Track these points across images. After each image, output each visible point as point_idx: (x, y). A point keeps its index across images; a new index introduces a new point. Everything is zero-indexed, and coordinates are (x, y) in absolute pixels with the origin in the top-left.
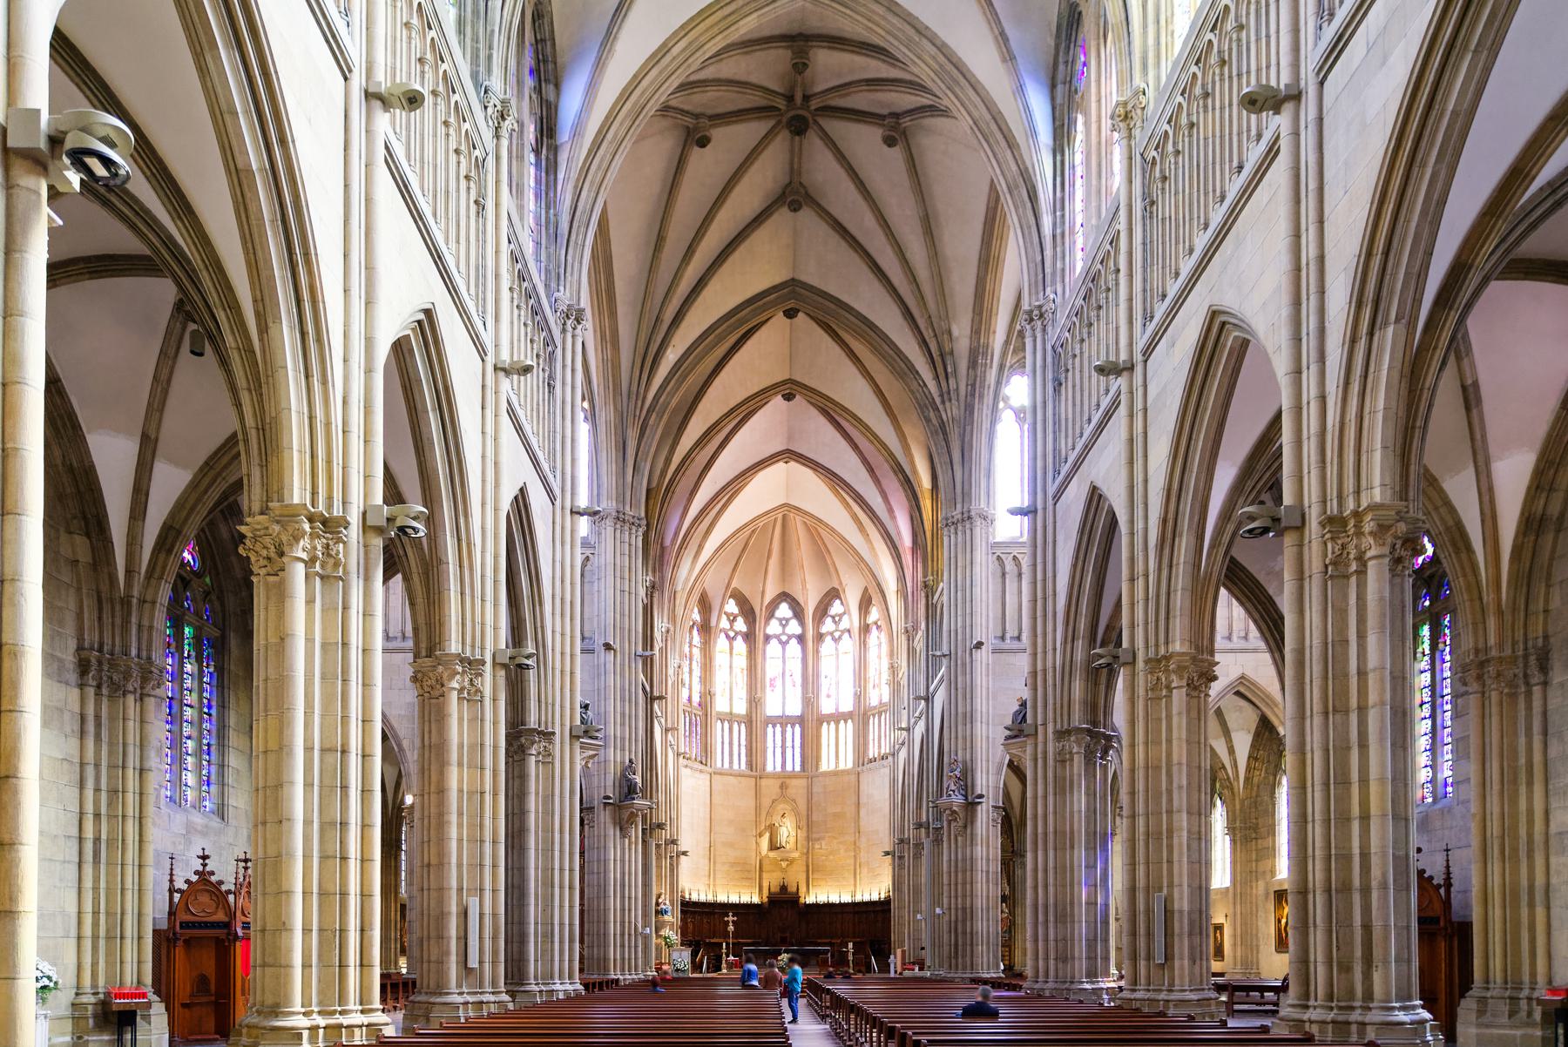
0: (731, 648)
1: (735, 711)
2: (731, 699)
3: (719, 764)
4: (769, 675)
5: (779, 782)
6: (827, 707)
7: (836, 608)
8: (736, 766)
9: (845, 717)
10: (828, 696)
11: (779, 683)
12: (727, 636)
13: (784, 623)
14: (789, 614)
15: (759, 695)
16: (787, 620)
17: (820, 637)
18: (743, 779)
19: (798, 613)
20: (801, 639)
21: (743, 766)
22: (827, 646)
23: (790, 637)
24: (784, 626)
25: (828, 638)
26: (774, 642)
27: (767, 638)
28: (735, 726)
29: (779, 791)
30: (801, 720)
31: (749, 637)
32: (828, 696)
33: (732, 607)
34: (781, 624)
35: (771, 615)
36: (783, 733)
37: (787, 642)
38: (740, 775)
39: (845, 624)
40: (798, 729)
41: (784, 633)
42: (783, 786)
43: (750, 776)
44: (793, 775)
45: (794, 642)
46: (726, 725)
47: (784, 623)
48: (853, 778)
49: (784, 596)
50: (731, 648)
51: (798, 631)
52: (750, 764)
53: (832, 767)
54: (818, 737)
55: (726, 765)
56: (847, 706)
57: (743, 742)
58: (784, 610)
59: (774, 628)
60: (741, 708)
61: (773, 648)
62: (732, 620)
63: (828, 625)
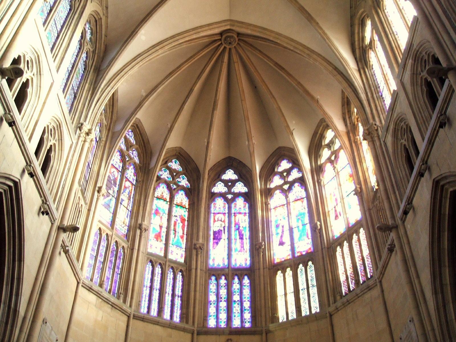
1: (170, 256)
3: (144, 310)
4: (215, 227)
8: (167, 315)
10: (282, 243)
11: (224, 236)
14: (234, 177)
15: (201, 241)
16: (233, 183)
17: (268, 193)
18: (174, 332)
20: (249, 197)
21: (177, 318)
22: (278, 198)
23: (237, 195)
24: (230, 188)
25: (278, 192)
26: (219, 202)
27: (213, 196)
28: (170, 275)
32: (282, 243)
33: (175, 165)
35: (217, 177)
37: (233, 200)
38: (170, 325)
40: (246, 281)
43: (184, 330)
45: (240, 202)
46: (158, 270)
48: (325, 323)
51: (244, 190)
52: (184, 316)
55: (154, 312)
58: (230, 175)
59: (219, 188)
61: (219, 204)
63: (277, 181)
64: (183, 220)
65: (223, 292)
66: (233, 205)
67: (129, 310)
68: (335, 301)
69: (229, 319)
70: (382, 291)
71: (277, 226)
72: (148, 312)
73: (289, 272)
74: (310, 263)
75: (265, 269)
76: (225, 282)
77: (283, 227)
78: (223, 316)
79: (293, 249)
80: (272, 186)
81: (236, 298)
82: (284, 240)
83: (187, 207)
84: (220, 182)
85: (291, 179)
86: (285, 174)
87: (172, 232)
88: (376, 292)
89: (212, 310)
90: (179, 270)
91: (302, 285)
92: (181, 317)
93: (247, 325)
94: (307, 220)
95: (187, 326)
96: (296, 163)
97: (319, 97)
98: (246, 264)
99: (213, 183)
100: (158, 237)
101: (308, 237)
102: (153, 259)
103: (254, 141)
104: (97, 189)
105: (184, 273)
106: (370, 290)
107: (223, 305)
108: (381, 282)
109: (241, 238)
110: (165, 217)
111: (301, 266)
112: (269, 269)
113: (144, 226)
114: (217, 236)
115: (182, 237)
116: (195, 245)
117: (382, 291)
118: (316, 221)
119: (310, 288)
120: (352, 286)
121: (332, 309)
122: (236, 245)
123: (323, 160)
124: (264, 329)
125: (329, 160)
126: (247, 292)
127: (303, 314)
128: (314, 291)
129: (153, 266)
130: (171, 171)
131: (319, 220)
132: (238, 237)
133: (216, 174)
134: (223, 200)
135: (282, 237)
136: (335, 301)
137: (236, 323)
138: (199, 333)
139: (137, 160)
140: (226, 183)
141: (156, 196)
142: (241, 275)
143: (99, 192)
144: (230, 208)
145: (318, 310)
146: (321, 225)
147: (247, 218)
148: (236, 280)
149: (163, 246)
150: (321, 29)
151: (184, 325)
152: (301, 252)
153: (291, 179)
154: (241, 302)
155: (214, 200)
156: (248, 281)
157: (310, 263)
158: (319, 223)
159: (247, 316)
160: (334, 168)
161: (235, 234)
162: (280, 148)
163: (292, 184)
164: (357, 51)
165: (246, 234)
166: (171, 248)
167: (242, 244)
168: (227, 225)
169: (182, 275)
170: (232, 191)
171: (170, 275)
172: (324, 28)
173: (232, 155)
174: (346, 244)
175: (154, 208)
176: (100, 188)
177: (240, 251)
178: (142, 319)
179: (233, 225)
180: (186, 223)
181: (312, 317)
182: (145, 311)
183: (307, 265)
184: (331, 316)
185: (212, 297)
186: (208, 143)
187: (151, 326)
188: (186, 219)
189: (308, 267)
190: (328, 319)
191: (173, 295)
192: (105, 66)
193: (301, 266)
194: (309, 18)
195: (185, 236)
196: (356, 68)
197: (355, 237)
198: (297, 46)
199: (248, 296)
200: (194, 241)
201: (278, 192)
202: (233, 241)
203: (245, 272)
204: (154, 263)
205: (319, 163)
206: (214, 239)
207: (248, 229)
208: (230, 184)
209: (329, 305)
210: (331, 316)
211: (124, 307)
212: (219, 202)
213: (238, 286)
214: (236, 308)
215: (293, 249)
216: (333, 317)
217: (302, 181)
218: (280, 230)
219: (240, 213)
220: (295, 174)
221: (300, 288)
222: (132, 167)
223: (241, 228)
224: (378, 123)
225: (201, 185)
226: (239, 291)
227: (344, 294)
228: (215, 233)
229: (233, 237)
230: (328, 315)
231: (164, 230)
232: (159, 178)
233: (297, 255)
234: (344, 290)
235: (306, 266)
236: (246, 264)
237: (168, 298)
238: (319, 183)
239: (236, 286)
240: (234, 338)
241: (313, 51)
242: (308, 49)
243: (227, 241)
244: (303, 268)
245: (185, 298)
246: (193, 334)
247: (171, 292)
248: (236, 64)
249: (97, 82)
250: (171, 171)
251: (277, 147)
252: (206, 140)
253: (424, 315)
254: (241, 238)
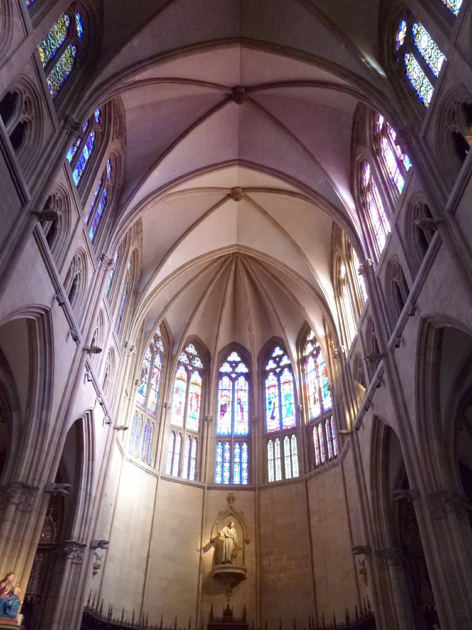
0: (189, 378)
2: (185, 417)
4: (222, 401)
5: (226, 493)
6: (272, 426)
7: (278, 352)
8: (184, 476)
9: (289, 432)
10: (273, 418)
12: (187, 369)
13: (234, 365)
14: (238, 359)
15: (211, 414)
16: (237, 363)
17: (264, 374)
19: (246, 359)
20: (248, 376)
21: (192, 478)
23: (239, 375)
24: (234, 368)
25: (271, 374)
26: (226, 380)
27: (220, 375)
28: (187, 442)
29: (226, 502)
30: (248, 439)
31: (205, 373)
33: (191, 349)
34: (231, 366)
35: (223, 359)
36: (231, 450)
37: (237, 378)
39: (285, 361)
40: (245, 446)
41: (234, 372)
42: (230, 499)
43: (198, 486)
44: (240, 488)
45: (242, 379)
46: (178, 439)
47: (234, 365)
48: (301, 486)
49: (235, 347)
50: (189, 378)
52: (198, 475)
53: (279, 478)
54: (265, 452)
55: (175, 474)
56: (290, 421)
57: (193, 455)
58: (234, 357)
59: (226, 368)
60: (193, 425)
61: (225, 382)
62: (191, 357)
63: (271, 365)
64: (197, 396)
65: (227, 455)
66: (236, 383)
67: (158, 473)
68: (310, 471)
69: (231, 477)
70: (343, 470)
71: (270, 403)
72: (171, 473)
73: (278, 441)
74: (293, 436)
75: (259, 439)
76: (229, 447)
77: (274, 404)
78: (227, 474)
79: (281, 424)
80: (268, 368)
81: (237, 460)
82: (274, 415)
83: (201, 385)
84: (226, 363)
85: (282, 364)
86: (277, 359)
87: (189, 407)
88: (338, 469)
89: (219, 469)
90: (194, 438)
91: (287, 453)
92: (196, 476)
93: (245, 482)
94: (293, 400)
95: (200, 484)
96: (286, 352)
97: (305, 305)
98: (245, 432)
99: (220, 365)
100: (178, 411)
101: (292, 414)
102: (174, 429)
103: (254, 333)
104: (135, 382)
105: (198, 440)
106: (334, 467)
107: (227, 465)
108: (342, 463)
109: (242, 411)
110: (184, 394)
111: (286, 437)
112: (262, 438)
113: (168, 405)
114: (224, 409)
115: (196, 411)
116: (207, 417)
117: (343, 470)
118: (299, 404)
119: (293, 456)
120: (323, 460)
121: (307, 475)
122: (238, 417)
123: (307, 352)
124: (257, 486)
125: (312, 354)
126: (245, 455)
127: (287, 478)
128: (295, 459)
129: (175, 435)
130: (188, 355)
131: (302, 404)
132: (239, 410)
133: (223, 356)
134: (228, 379)
135: (273, 412)
136: (310, 471)
137: (236, 481)
138: (209, 488)
139: (162, 349)
140: (231, 363)
141: (176, 377)
142: (241, 441)
143: (136, 384)
144: (234, 386)
145: (298, 476)
146: (302, 407)
147: (246, 394)
148: (237, 446)
149: (183, 418)
150: (308, 261)
151: (197, 482)
152: (287, 426)
153: (282, 364)
154: (241, 463)
155: (221, 379)
156: (246, 447)
157: (293, 436)
158: (301, 406)
159: (245, 474)
160: (315, 362)
161: (237, 408)
162: (274, 337)
163: (283, 368)
164: (335, 281)
165: (246, 408)
166: (188, 420)
167: (243, 415)
168: (231, 400)
169: (197, 442)
170: (236, 371)
171: (187, 442)
172: (310, 261)
173: (236, 341)
174: (320, 425)
175: (175, 387)
176: (137, 381)
177: (241, 422)
178: (168, 479)
179: (236, 400)
180: (200, 398)
181: (293, 481)
182: (169, 474)
183: (291, 437)
184: (306, 481)
185: (219, 459)
186: (218, 334)
187: (173, 484)
188: (200, 395)
189: (292, 439)
190: (304, 482)
191: (190, 458)
192: (141, 290)
193: (286, 437)
194: (299, 251)
195: (199, 409)
196: (333, 296)
197: (327, 422)
198: (289, 271)
199: (246, 459)
200: (206, 414)
201: (271, 374)
202: (236, 413)
203: (244, 440)
204: (175, 432)
205: (304, 355)
206: (221, 411)
207: (247, 403)
208: (234, 365)
209: (306, 473)
210: (306, 481)
211: (155, 472)
212: (226, 380)
213: (239, 451)
214: (237, 469)
215: (281, 424)
216: (308, 482)
217: (290, 367)
218: (272, 406)
219: (242, 390)
220: (285, 361)
221: (285, 455)
222: (158, 355)
223: (242, 403)
224: (345, 347)
225: (211, 367)
226: (239, 454)
227: (317, 465)
228: (222, 406)
229: (235, 410)
230: (304, 480)
231: (183, 405)
232: (179, 362)
233: (284, 428)
234: (317, 461)
235: (290, 438)
236: (245, 432)
237: (186, 461)
238: (303, 371)
239: (237, 451)
240: (235, 493)
241: (301, 277)
242: (297, 274)
243: (231, 413)
244: (288, 440)
245: (199, 460)
246: (204, 489)
247: (188, 455)
248: (241, 273)
249: (137, 304)
250: (188, 355)
251: (272, 336)
252: (216, 331)
253: (365, 503)
254: (242, 411)
